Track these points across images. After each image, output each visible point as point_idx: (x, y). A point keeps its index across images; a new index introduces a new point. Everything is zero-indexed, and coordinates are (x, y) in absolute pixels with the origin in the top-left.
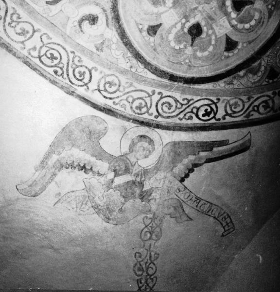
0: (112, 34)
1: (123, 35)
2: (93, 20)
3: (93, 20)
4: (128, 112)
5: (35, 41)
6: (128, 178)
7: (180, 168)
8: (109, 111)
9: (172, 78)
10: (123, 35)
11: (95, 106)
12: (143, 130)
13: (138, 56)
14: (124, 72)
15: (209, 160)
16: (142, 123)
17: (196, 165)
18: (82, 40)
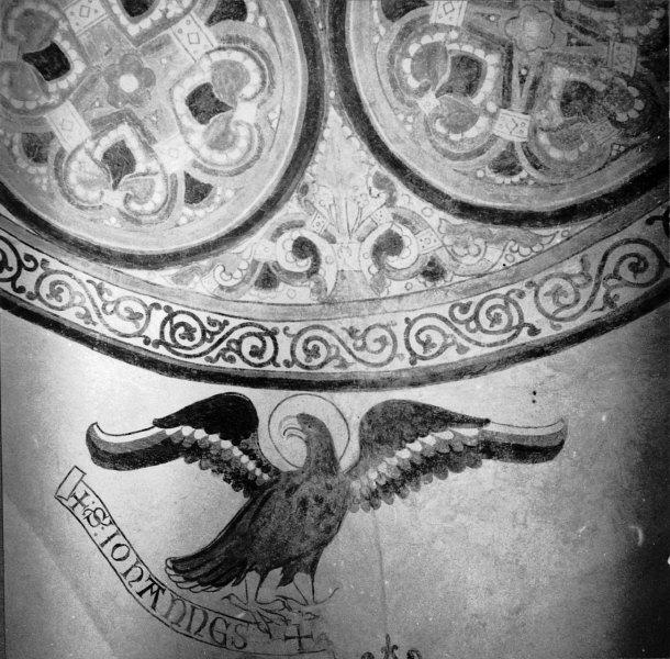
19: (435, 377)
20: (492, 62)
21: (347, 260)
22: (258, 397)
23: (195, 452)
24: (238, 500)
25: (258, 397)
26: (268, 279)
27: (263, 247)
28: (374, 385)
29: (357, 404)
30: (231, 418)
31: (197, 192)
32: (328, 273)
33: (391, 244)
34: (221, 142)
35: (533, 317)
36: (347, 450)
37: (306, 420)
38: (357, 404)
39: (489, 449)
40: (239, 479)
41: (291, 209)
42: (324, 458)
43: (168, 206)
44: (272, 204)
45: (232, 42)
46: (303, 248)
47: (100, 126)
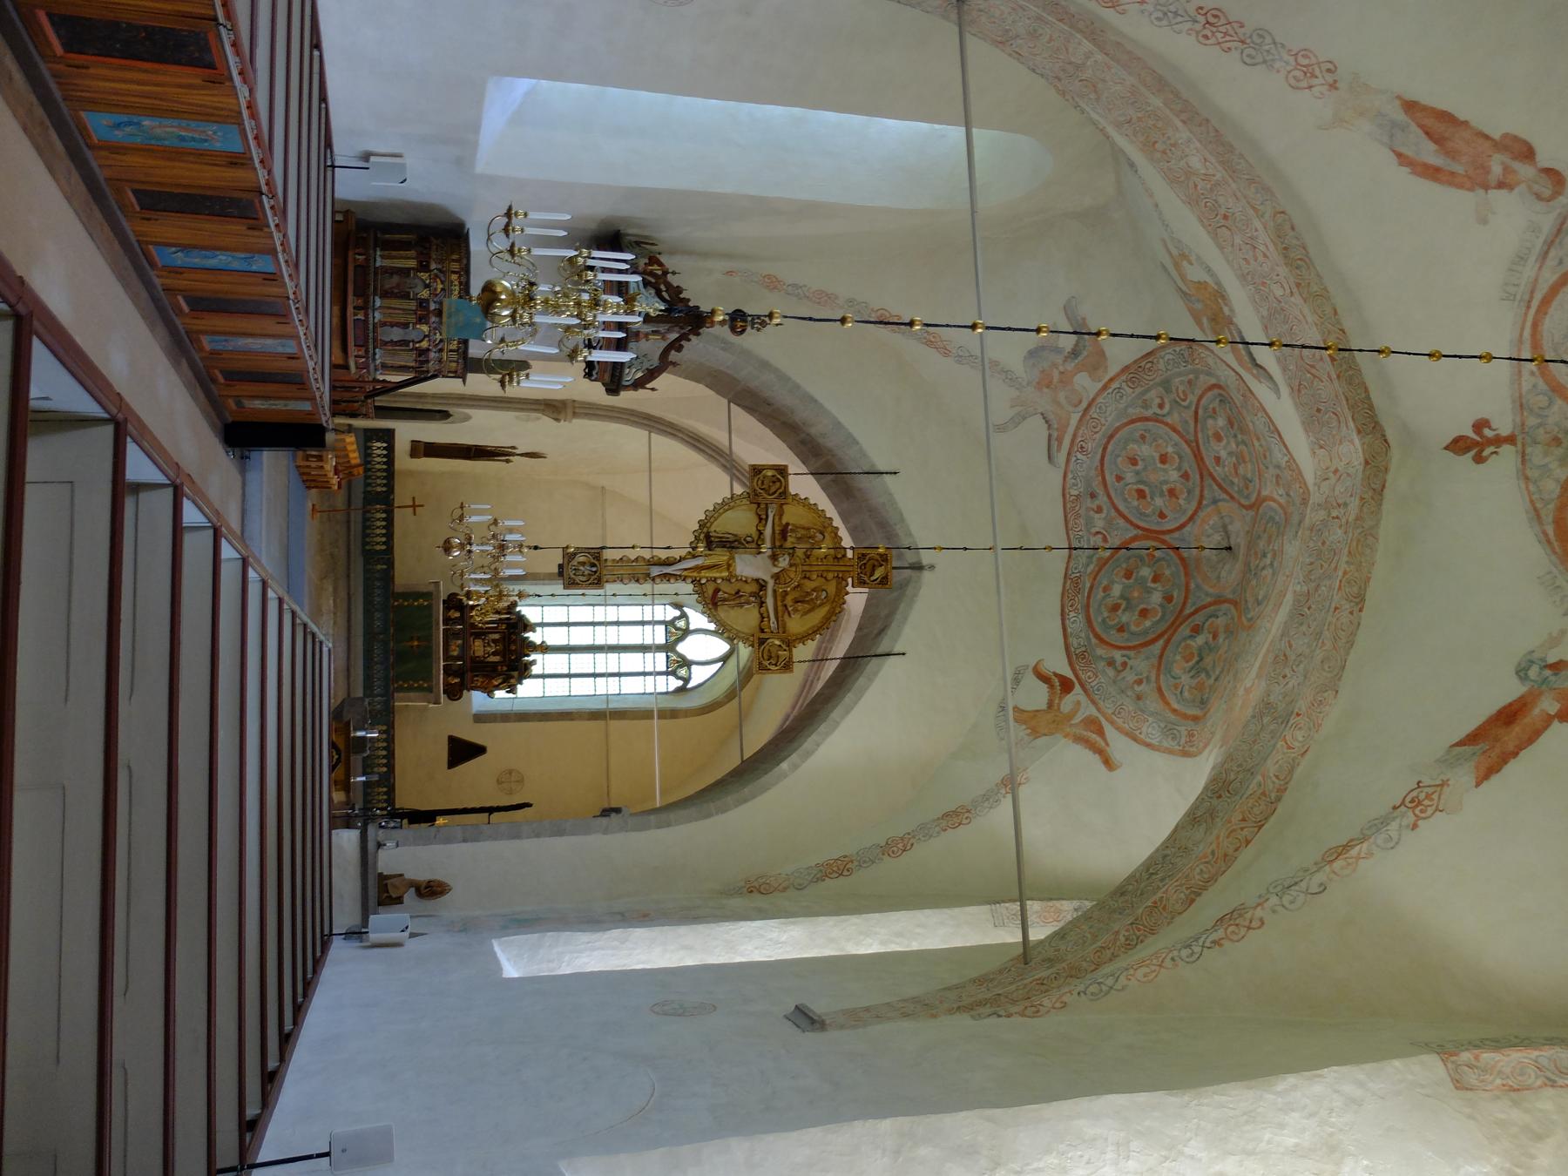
0: (1149, 413)
1: (1147, 419)
2: (1161, 406)
3: (1161, 406)
4: (1100, 400)
5: (1161, 365)
6: (1055, 380)
7: (1051, 417)
8: (1105, 387)
9: (1111, 437)
10: (1147, 419)
11: (1111, 380)
12: (1084, 404)
13: (1132, 422)
14: (1126, 408)
15: (1050, 436)
16: (1089, 405)
17: (1049, 427)
18: (1153, 394)
19: (1112, 723)
20: (1196, 659)
21: (1130, 677)
22: (1077, 686)
23: (1052, 686)
24: (1044, 707)
25: (1077, 686)
26: (1111, 663)
27: (1118, 656)
28: (1099, 710)
29: (1093, 711)
30: (1067, 686)
31: (1121, 629)
32: (1123, 674)
33: (1139, 682)
34: (1138, 625)
35: (1144, 729)
36: (1076, 721)
37: (1079, 703)
38: (1093, 711)
39: (1100, 752)
40: (1050, 705)
41: (1131, 653)
42: (1070, 716)
43: (1112, 627)
44: (1129, 648)
45: (1161, 605)
46: (1124, 664)
47: (1122, 597)
